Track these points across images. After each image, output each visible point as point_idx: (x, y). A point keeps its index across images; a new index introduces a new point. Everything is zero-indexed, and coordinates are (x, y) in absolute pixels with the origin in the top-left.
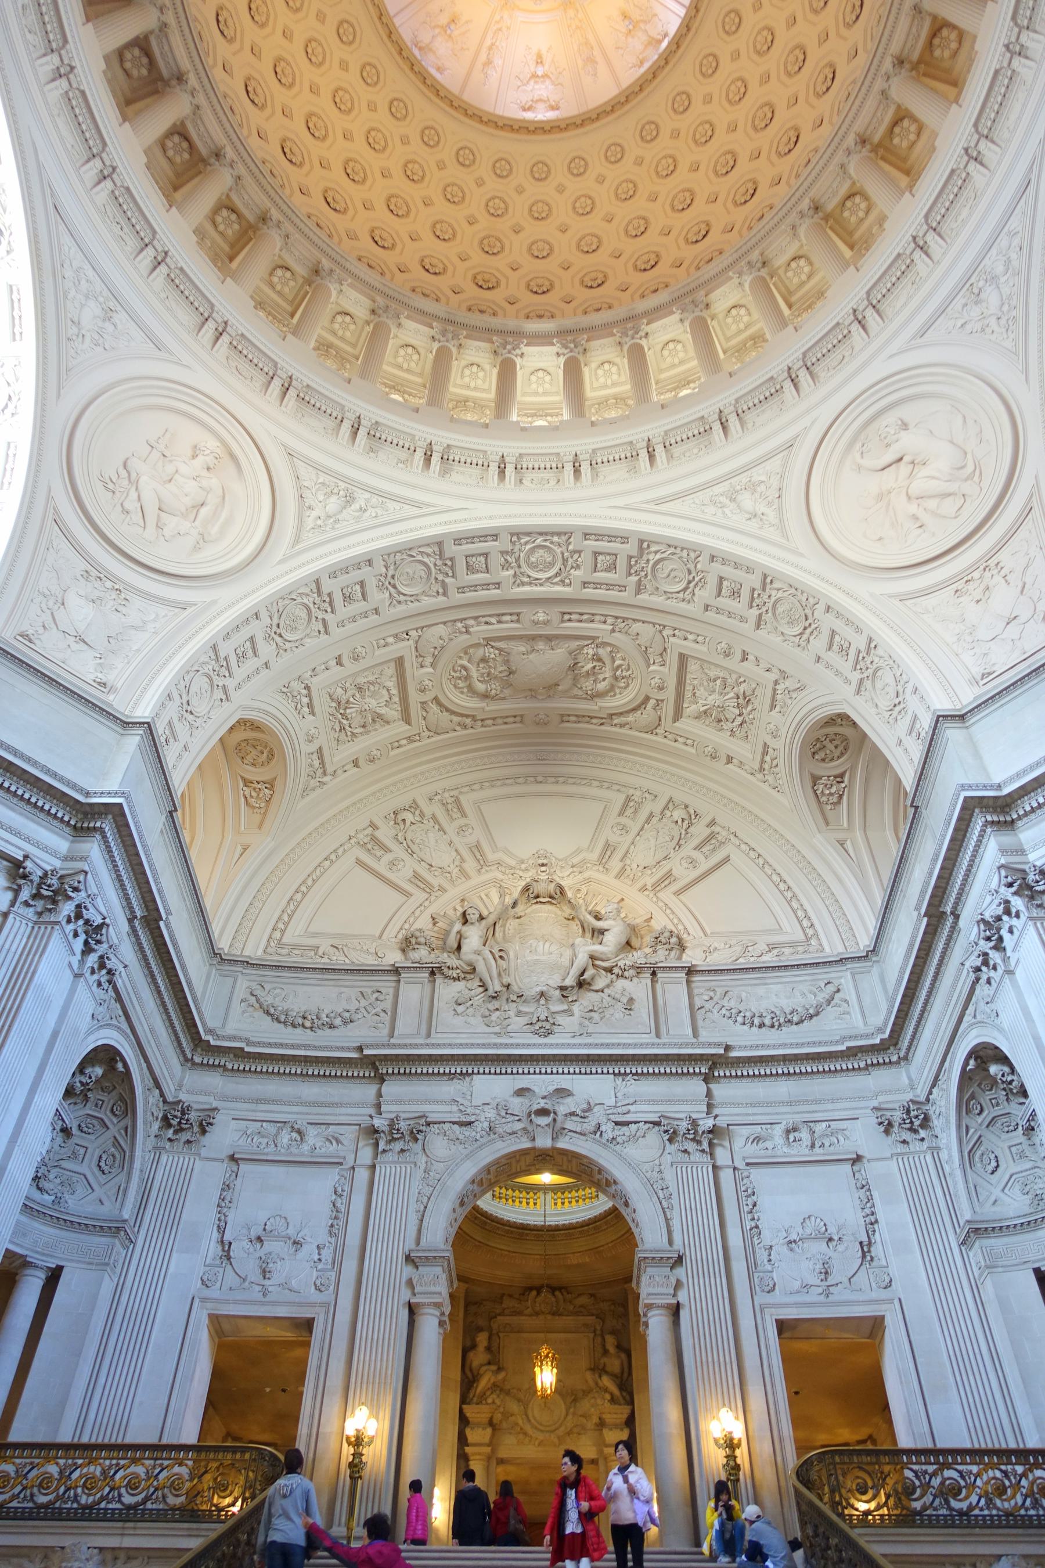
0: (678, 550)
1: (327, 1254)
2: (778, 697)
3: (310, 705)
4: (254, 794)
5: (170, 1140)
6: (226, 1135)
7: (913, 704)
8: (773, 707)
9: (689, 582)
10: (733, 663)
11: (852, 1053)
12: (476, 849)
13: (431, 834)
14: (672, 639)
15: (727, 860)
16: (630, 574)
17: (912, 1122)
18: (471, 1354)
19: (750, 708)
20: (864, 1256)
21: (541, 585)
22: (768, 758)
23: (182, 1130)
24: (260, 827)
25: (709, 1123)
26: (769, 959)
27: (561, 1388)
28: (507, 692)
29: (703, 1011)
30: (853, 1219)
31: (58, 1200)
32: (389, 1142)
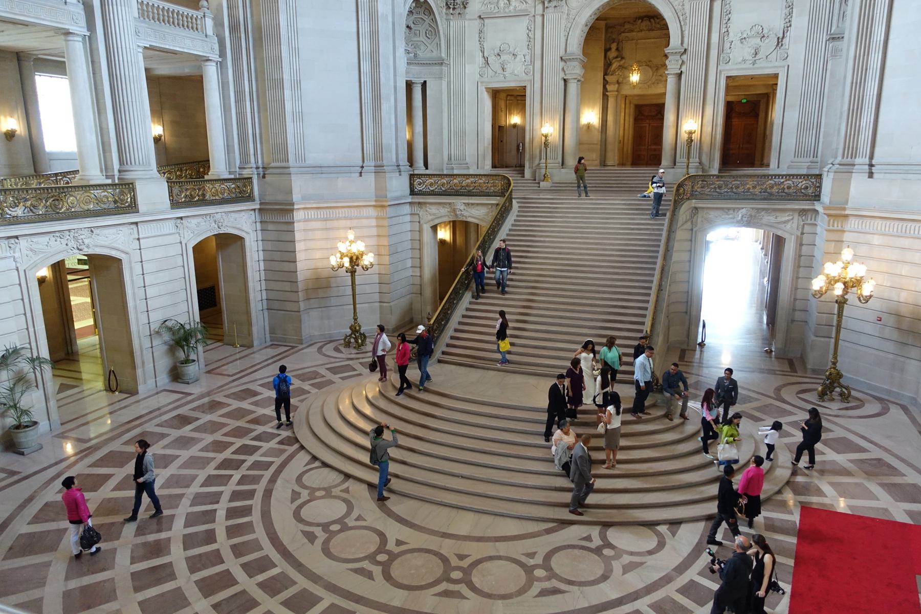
1: (528, 58)
18: (609, 53)
27: (641, 81)
30: (778, 24)
31: (415, 55)
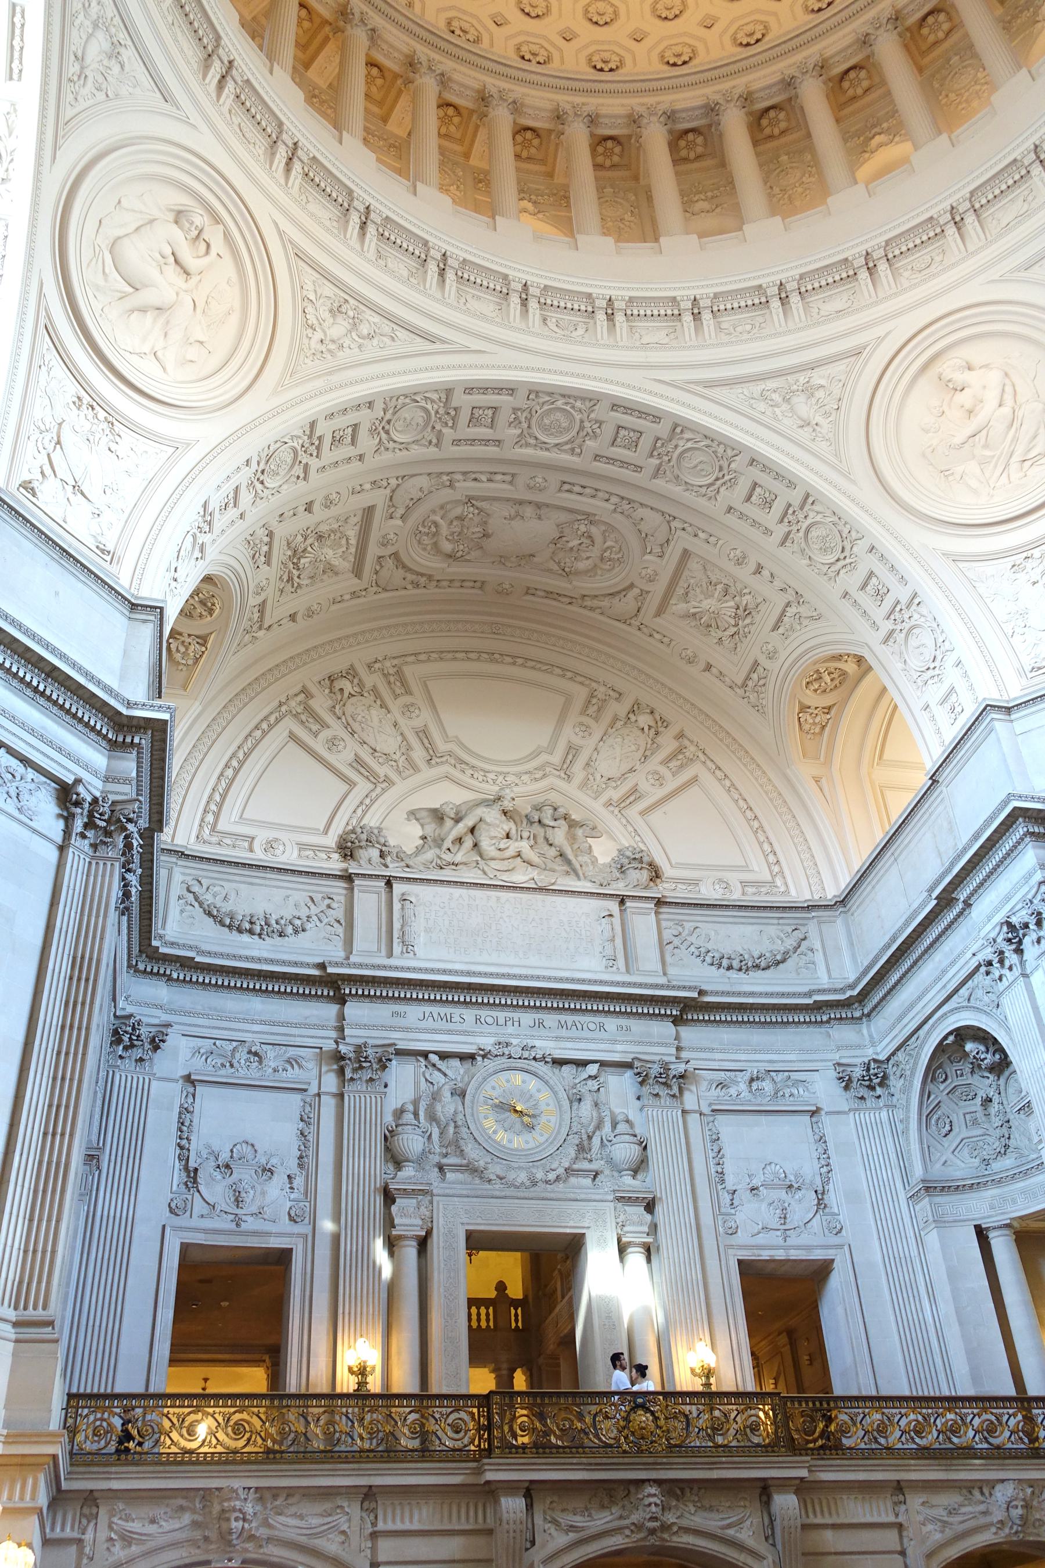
0: (715, 444)
1: (299, 1182)
2: (786, 619)
3: (268, 555)
4: (182, 649)
5: (121, 1057)
6: (179, 1054)
7: (951, 676)
8: (776, 627)
9: (717, 479)
10: (744, 574)
11: (818, 1007)
12: (423, 734)
13: (373, 712)
14: (680, 533)
15: (695, 780)
16: (651, 456)
17: (870, 1080)
19: (748, 621)
20: (819, 1204)
21: (547, 449)
22: (755, 676)
23: (132, 1046)
24: (185, 687)
25: (681, 1068)
26: (736, 896)
28: (474, 554)
29: (671, 946)
30: (809, 1169)
32: (355, 1070)
